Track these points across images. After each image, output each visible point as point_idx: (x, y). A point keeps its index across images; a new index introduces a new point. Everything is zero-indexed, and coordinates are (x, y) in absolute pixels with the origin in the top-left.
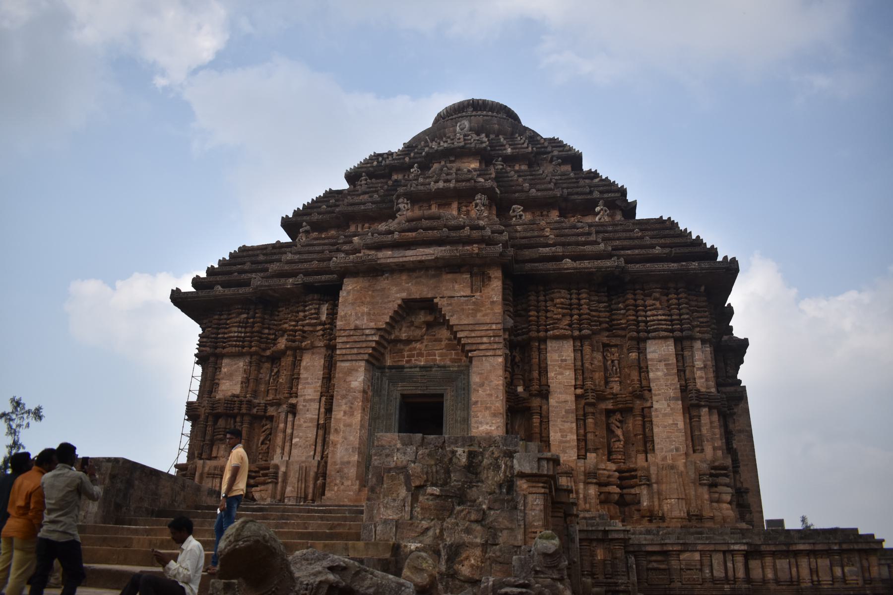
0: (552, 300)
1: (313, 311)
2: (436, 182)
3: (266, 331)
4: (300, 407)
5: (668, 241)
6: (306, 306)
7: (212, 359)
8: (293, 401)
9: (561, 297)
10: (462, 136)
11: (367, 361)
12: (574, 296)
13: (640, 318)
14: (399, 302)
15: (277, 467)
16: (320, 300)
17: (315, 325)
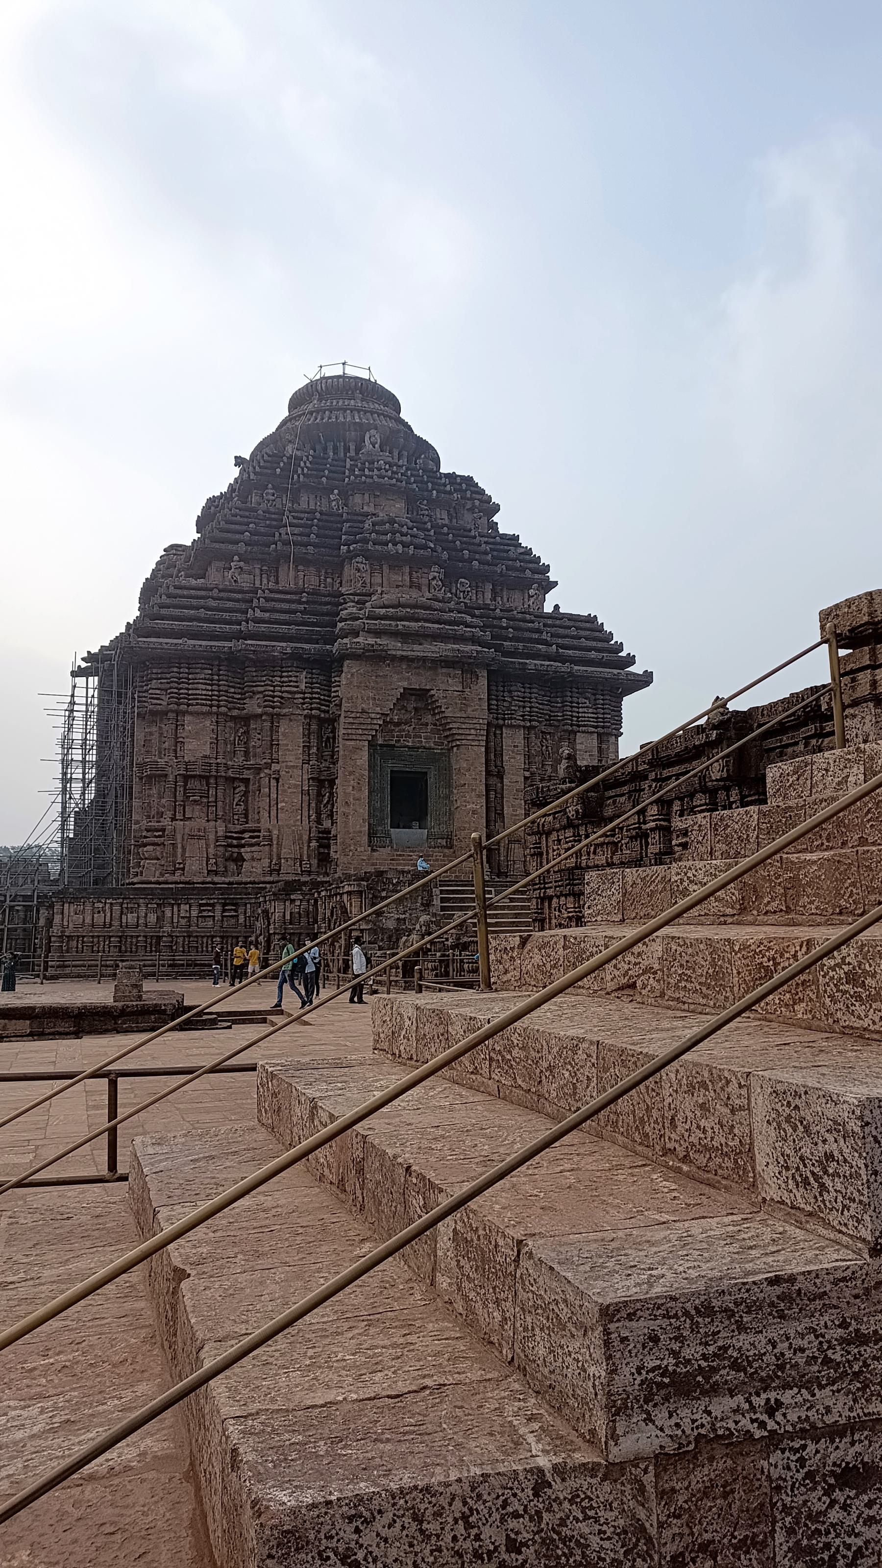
0: (510, 692)
1: (293, 679)
2: (395, 544)
3: (232, 690)
4: (282, 773)
5: (599, 645)
6: (283, 672)
7: (171, 715)
8: (275, 767)
9: (518, 690)
10: (387, 467)
11: (369, 741)
12: (528, 690)
13: (574, 714)
14: (402, 691)
15: (269, 831)
16: (297, 667)
17: (295, 693)
